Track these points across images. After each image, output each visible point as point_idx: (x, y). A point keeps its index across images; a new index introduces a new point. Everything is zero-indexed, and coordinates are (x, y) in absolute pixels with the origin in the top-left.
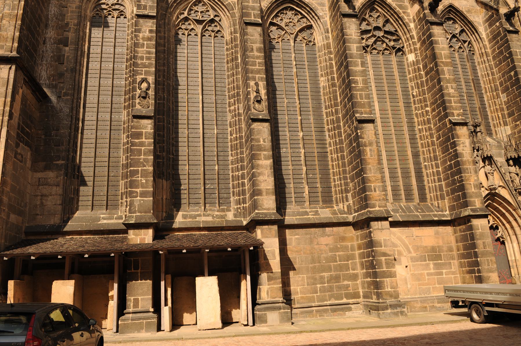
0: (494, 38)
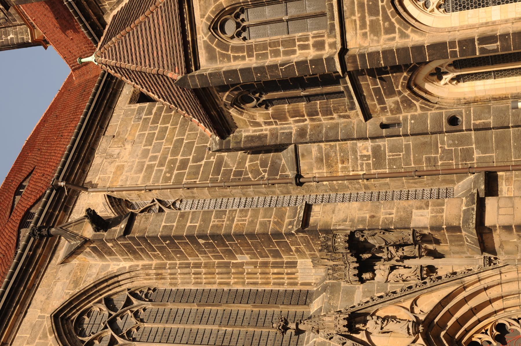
0: (134, 252)
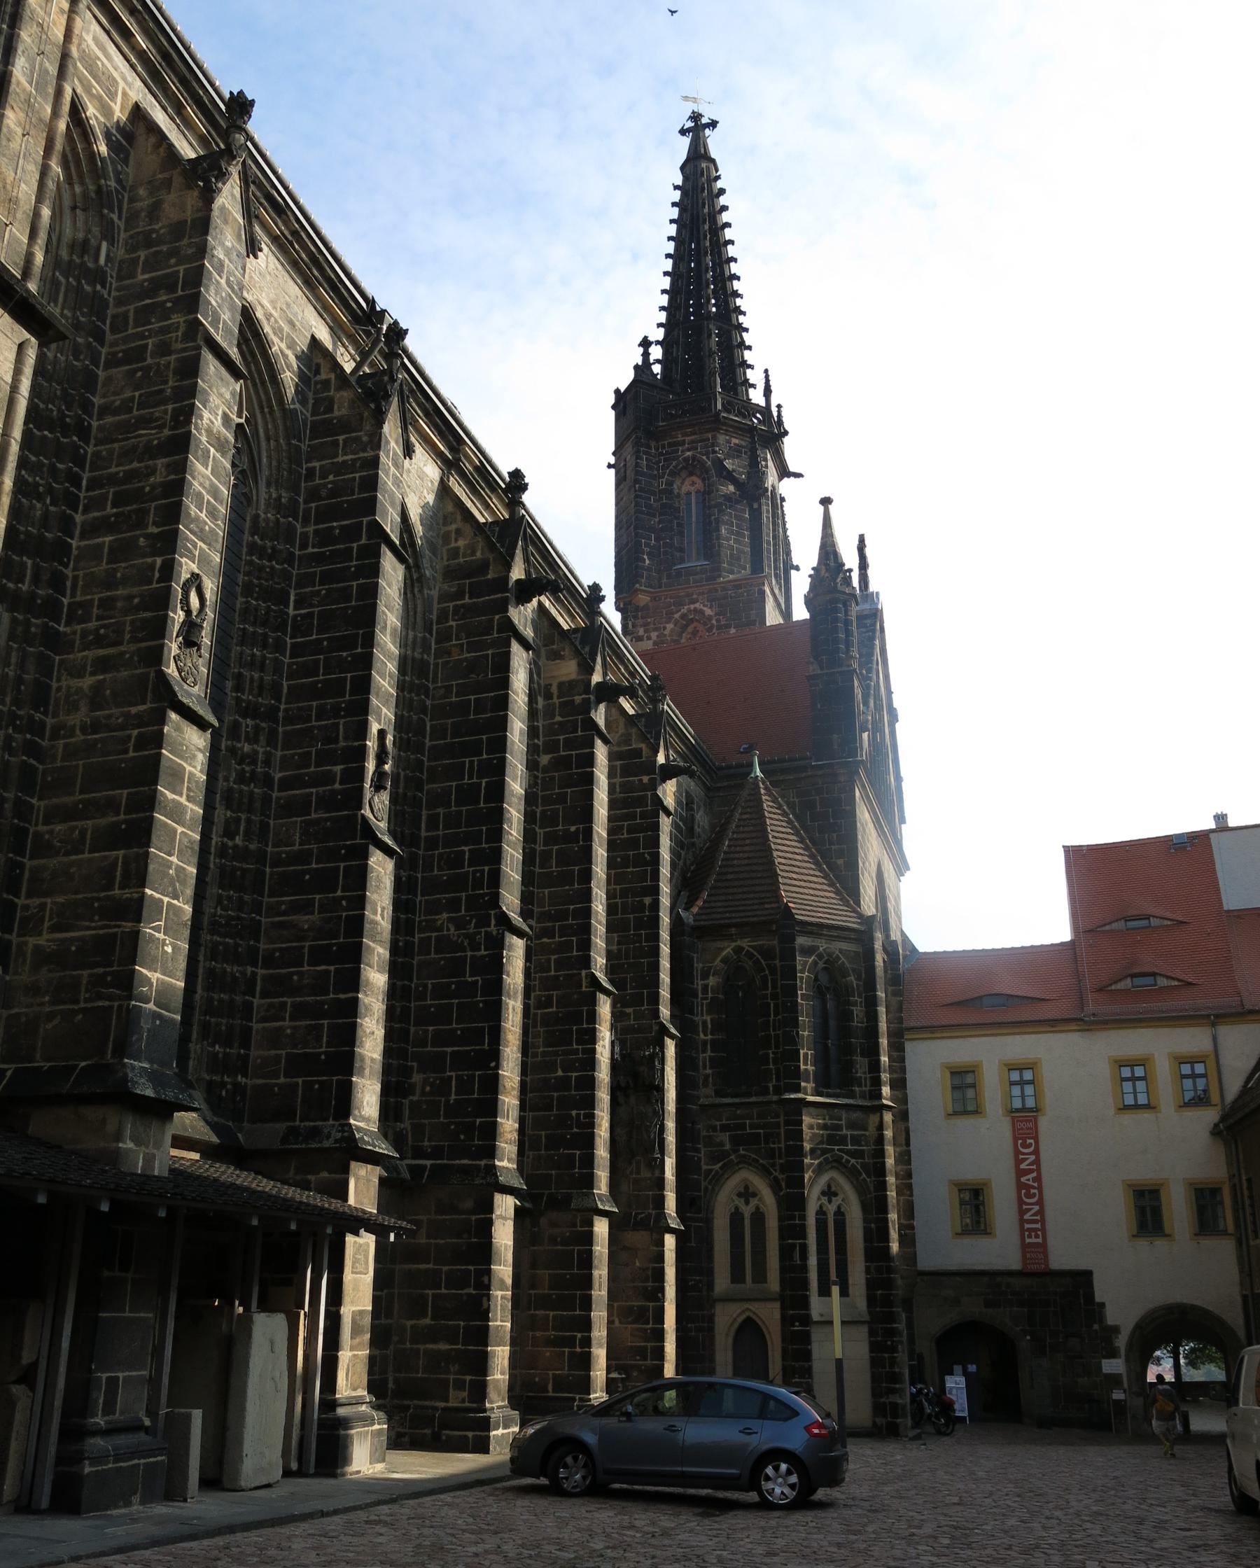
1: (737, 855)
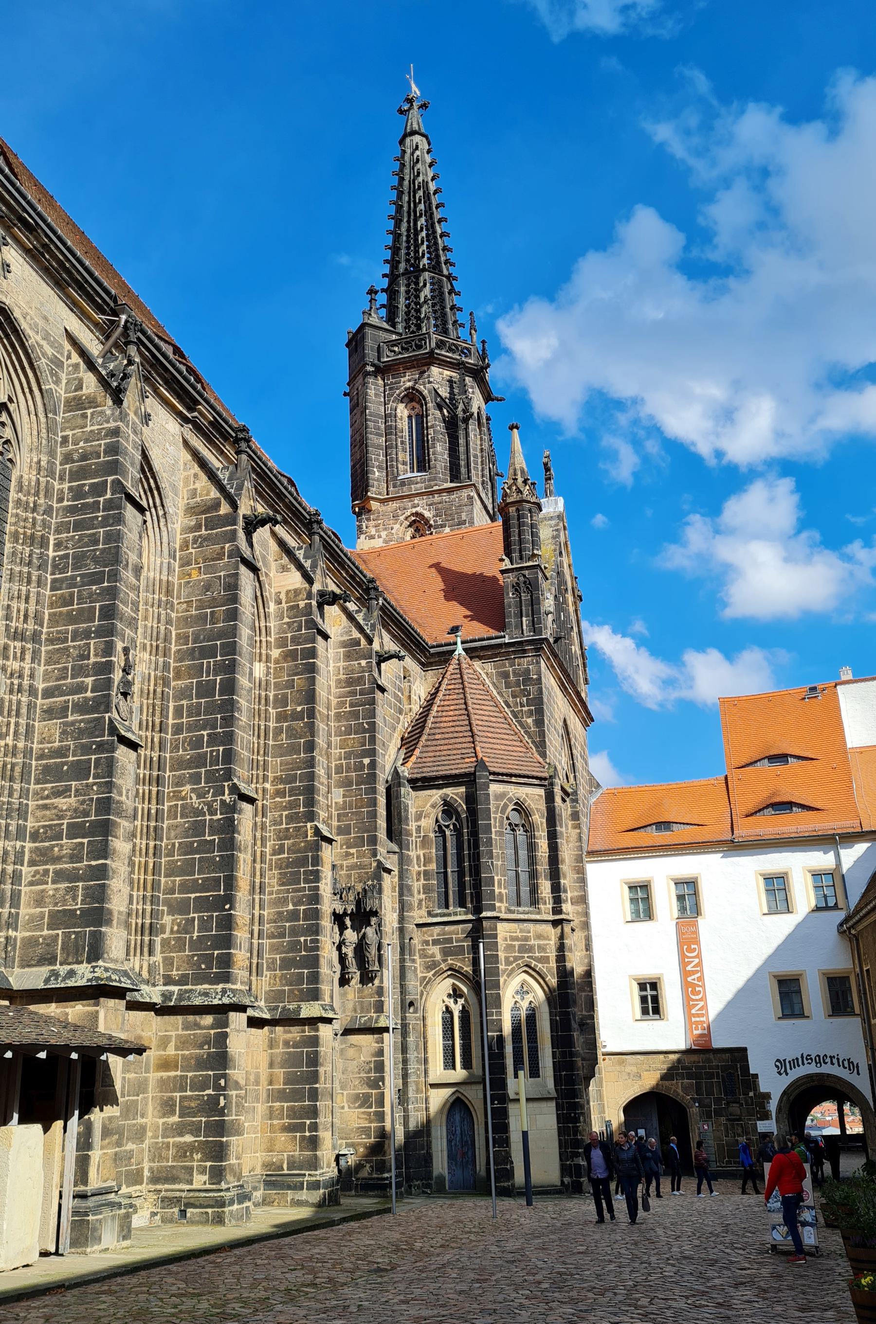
0: (350, 682)
1: (444, 719)
